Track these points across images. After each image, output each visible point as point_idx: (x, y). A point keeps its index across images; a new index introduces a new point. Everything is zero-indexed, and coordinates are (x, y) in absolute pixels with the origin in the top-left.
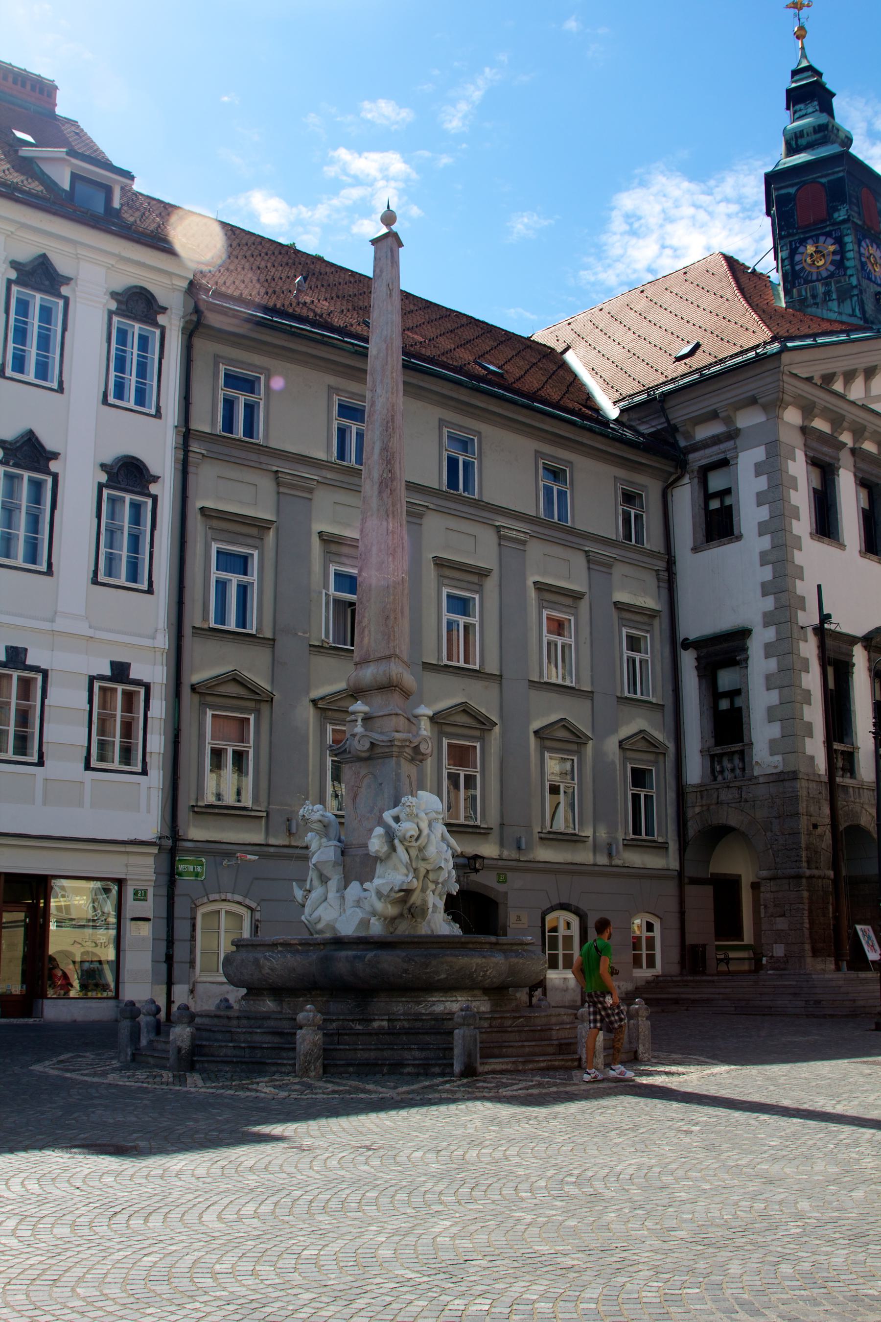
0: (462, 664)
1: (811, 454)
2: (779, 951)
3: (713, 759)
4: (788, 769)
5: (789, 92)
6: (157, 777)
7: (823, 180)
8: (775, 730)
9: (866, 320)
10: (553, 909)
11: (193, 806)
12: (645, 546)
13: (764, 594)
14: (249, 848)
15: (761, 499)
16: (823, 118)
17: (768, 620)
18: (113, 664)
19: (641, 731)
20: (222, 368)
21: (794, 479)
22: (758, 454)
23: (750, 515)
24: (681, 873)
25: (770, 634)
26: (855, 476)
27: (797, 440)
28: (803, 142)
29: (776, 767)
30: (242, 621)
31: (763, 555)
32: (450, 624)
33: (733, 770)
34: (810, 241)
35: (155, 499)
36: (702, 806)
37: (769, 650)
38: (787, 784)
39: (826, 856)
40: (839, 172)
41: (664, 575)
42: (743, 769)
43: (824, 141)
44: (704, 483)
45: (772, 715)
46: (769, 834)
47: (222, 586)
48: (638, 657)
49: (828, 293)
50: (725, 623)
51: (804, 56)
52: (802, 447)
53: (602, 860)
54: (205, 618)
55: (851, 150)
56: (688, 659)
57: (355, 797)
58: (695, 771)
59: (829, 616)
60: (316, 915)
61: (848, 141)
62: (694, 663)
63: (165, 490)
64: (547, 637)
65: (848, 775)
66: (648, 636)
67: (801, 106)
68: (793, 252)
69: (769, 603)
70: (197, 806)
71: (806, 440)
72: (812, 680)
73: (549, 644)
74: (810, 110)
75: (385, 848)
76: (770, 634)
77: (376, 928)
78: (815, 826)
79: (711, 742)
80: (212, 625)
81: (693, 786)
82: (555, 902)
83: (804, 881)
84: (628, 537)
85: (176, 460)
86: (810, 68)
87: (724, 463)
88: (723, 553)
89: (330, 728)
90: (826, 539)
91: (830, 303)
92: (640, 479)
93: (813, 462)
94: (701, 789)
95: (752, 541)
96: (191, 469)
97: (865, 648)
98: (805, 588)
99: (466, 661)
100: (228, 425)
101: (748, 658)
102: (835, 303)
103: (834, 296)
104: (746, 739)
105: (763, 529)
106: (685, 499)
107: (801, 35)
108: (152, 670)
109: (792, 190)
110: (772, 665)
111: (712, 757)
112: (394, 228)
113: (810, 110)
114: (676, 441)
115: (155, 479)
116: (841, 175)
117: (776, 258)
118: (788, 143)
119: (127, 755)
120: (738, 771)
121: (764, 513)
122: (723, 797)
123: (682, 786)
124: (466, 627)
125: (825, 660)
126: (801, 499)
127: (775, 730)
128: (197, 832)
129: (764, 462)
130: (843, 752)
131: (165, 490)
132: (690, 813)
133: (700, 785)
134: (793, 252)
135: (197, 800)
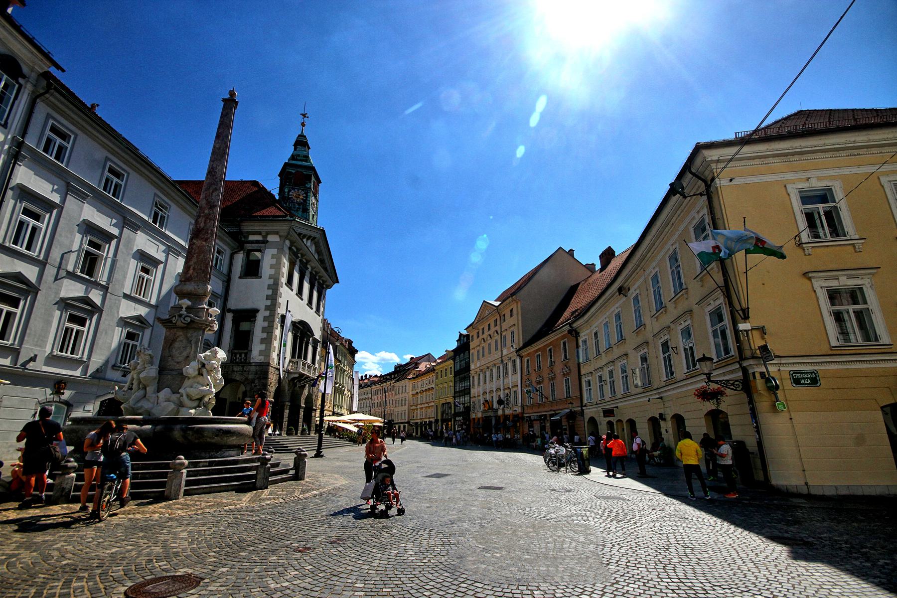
15: (272, 266)
17: (267, 308)
23: (266, 269)
25: (267, 313)
31: (269, 285)
37: (265, 319)
39: (272, 394)
43: (306, 161)
50: (249, 305)
60: (139, 405)
68: (289, 191)
69: (269, 303)
75: (197, 373)
76: (267, 313)
92: (225, 247)
98: (282, 301)
122: (235, 369)
126: (285, 270)
134: (289, 191)
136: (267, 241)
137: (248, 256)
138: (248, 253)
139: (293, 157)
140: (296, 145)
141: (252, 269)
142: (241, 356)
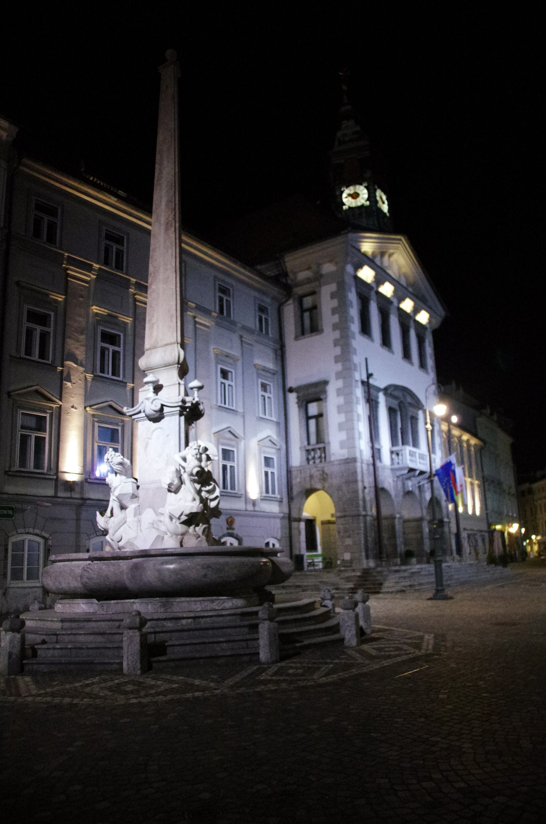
1: (359, 290)
2: (347, 556)
4: (351, 457)
8: (343, 436)
12: (270, 335)
14: (45, 499)
15: (334, 311)
19: (268, 437)
21: (351, 302)
22: (333, 287)
23: (328, 318)
25: (340, 383)
26: (377, 305)
27: (352, 282)
29: (344, 456)
38: (351, 464)
41: (279, 352)
44: (301, 303)
46: (340, 492)
47: (30, 333)
53: (250, 507)
54: (18, 350)
56: (292, 398)
57: (147, 446)
58: (297, 458)
60: (117, 537)
62: (296, 400)
69: (339, 367)
77: (170, 543)
78: (365, 488)
79: (306, 443)
80: (23, 355)
81: (296, 467)
83: (361, 518)
84: (261, 330)
87: (313, 293)
89: (96, 424)
90: (366, 336)
94: (300, 469)
95: (329, 335)
101: (326, 398)
104: (326, 441)
105: (335, 327)
106: (290, 311)
126: (354, 312)
127: (343, 436)
132: (294, 482)
135: (10, 467)
136: (321, 276)
137: (301, 303)
138: (300, 300)
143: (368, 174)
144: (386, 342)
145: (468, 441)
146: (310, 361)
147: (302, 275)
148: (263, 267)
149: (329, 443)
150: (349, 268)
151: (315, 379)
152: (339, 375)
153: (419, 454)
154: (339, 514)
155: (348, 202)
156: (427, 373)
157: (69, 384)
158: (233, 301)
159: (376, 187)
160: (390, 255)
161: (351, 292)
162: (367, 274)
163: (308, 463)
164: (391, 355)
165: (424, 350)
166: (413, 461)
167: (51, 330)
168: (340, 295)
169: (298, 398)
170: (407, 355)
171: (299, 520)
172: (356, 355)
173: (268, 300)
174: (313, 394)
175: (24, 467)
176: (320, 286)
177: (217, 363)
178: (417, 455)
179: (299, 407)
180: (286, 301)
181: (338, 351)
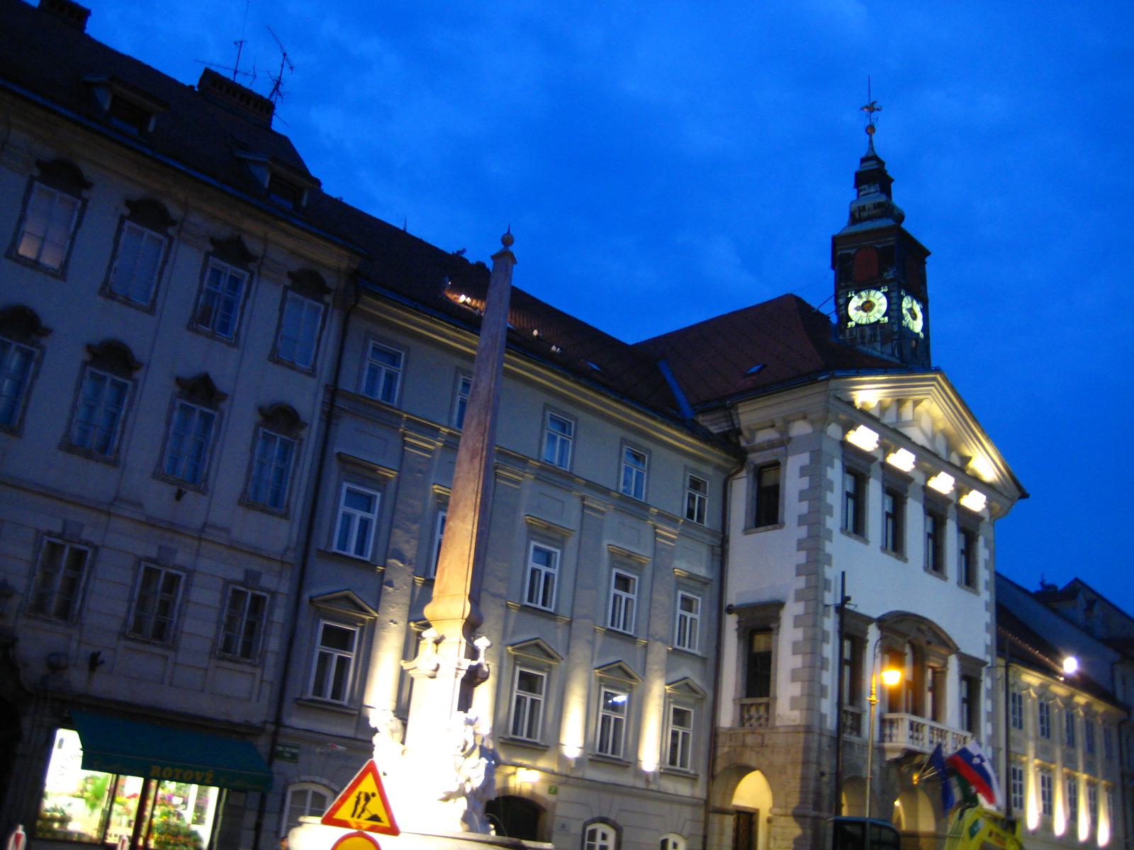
0: (539, 606)
1: (847, 464)
3: (743, 709)
5: (857, 175)
6: (271, 672)
7: (878, 246)
9: (901, 359)
10: (594, 821)
11: (298, 699)
12: (706, 524)
13: (797, 576)
15: (803, 496)
16: (883, 198)
17: (799, 596)
18: (247, 573)
20: (371, 342)
24: (707, 802)
27: (838, 452)
28: (864, 214)
29: (794, 720)
30: (361, 549)
32: (534, 571)
33: (759, 718)
34: (863, 294)
35: (302, 440)
36: (730, 747)
37: (798, 621)
40: (891, 240)
41: (718, 550)
42: (767, 720)
45: (795, 676)
47: (348, 518)
48: (689, 615)
49: (873, 336)
51: (872, 149)
52: (840, 457)
54: (330, 544)
55: (903, 225)
56: (731, 622)
58: (727, 717)
59: (849, 599)
61: (900, 218)
62: (735, 626)
63: (311, 436)
64: (613, 591)
65: (855, 733)
66: (699, 598)
67: (866, 187)
69: (801, 582)
70: (301, 699)
71: (844, 452)
72: (830, 651)
73: (615, 596)
74: (872, 190)
78: (822, 774)
79: (744, 693)
82: (596, 815)
85: (323, 412)
86: (875, 158)
88: (767, 536)
91: (875, 344)
93: (848, 470)
94: (731, 732)
95: (791, 531)
96: (334, 421)
97: (880, 627)
98: (831, 573)
99: (544, 604)
100: (371, 388)
101: (779, 627)
102: (879, 344)
103: (879, 338)
104: (772, 694)
105: (802, 520)
106: (741, 491)
107: (870, 129)
108: (277, 583)
109: (852, 252)
110: (799, 634)
111: (742, 706)
112: (511, 249)
113: (872, 190)
114: (739, 443)
115: (303, 425)
116: (892, 243)
117: (836, 303)
118: (852, 214)
119: (248, 650)
120: (763, 721)
121: (804, 507)
123: (715, 728)
124: (547, 576)
125: (843, 634)
126: (835, 499)
128: (297, 720)
129: (808, 466)
130: (852, 714)
131: (311, 436)
133: (730, 729)
135: (302, 694)
136: (790, 439)
138: (759, 472)
139: (854, 219)
140: (857, 186)
141: (766, 511)
142: (757, 710)
143: (889, 275)
144: (895, 544)
145: (1087, 706)
146: (762, 566)
147: (763, 436)
148: (707, 417)
149: (775, 698)
150: (833, 430)
151: (766, 596)
152: (799, 596)
153: (932, 728)
154: (777, 811)
155: (856, 315)
156: (976, 592)
157: (391, 589)
158: (648, 473)
159: (903, 293)
160: (916, 403)
161: (832, 466)
162: (864, 438)
163: (743, 725)
164: (899, 563)
165: (974, 556)
166: (917, 739)
167: (374, 517)
168: (814, 471)
169: (739, 622)
170: (936, 564)
171: (723, 812)
172: (830, 565)
173: (708, 470)
174: (760, 621)
175: (320, 695)
176: (786, 456)
177: (612, 565)
178: (926, 730)
179: (739, 637)
180: (738, 472)
181: (801, 557)
